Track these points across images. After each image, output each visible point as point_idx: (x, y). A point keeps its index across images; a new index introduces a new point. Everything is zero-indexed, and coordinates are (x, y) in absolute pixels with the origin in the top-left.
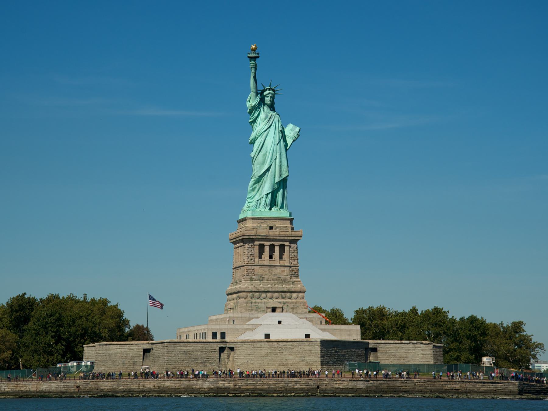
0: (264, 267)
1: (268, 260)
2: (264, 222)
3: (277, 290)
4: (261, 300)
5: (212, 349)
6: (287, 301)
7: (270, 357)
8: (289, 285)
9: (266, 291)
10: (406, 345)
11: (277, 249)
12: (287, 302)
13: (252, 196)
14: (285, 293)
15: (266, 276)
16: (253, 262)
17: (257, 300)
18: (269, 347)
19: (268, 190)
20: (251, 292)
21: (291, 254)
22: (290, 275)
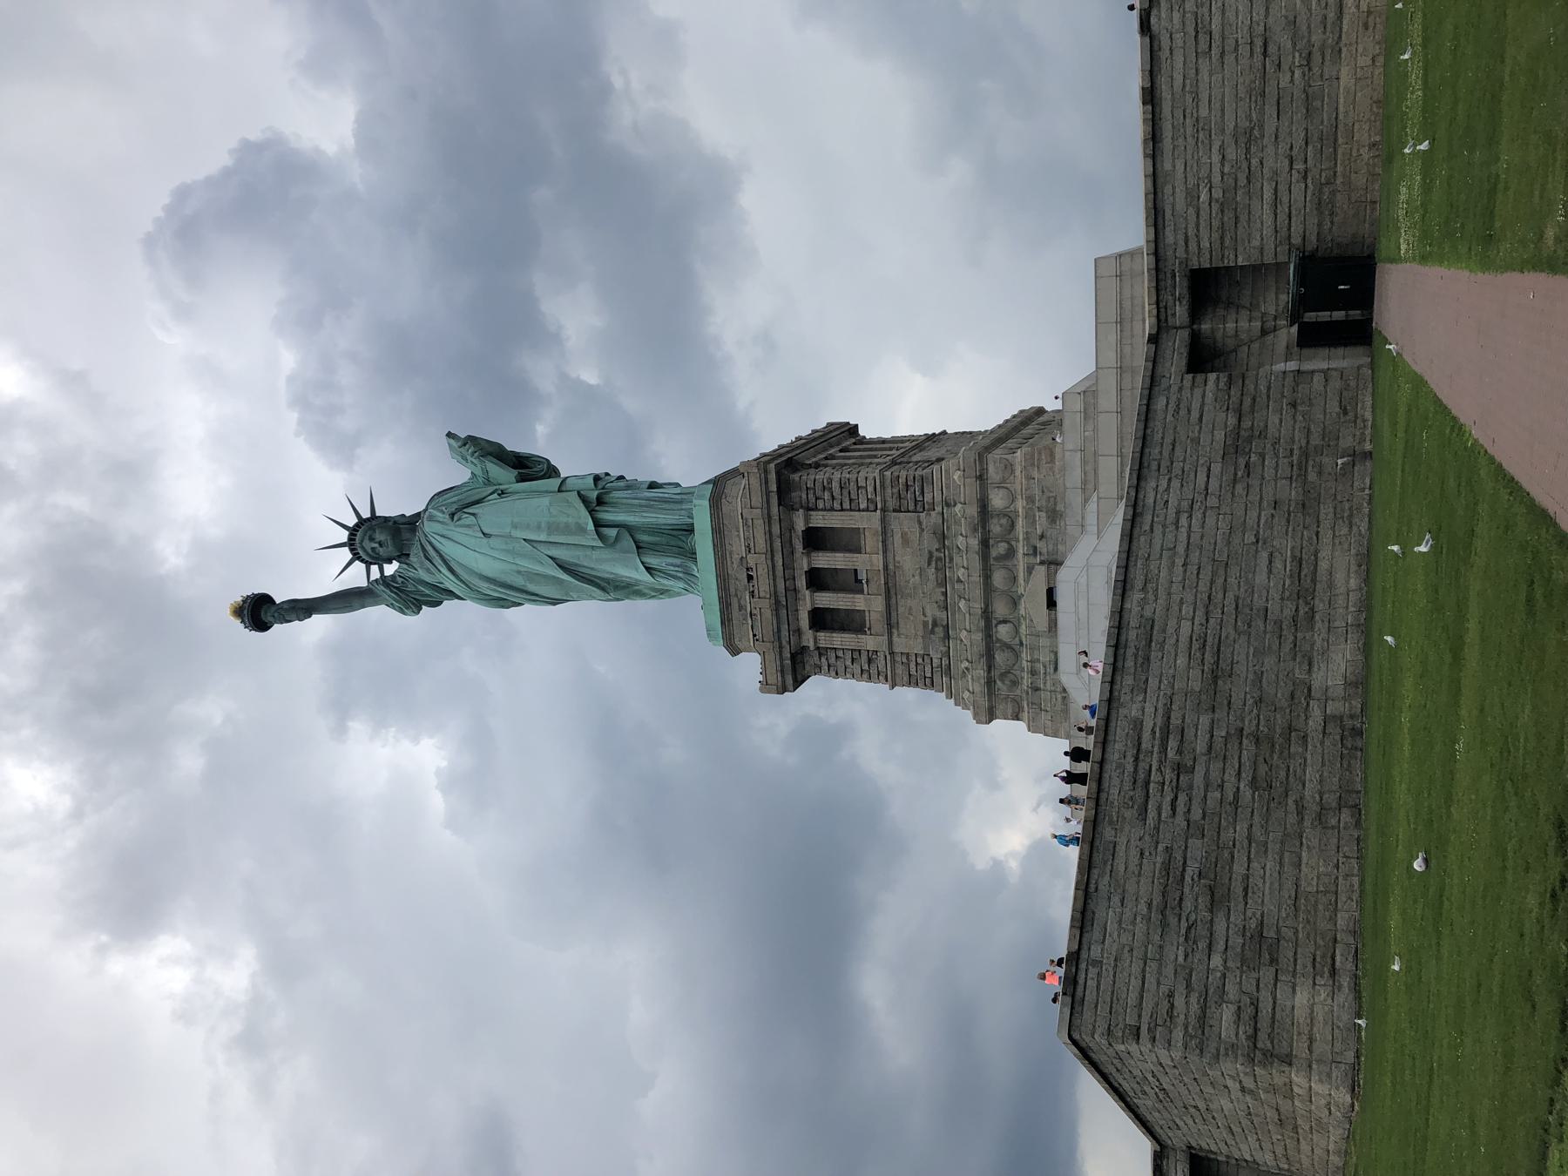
0: (894, 614)
1: (865, 600)
3: (976, 577)
4: (1021, 644)
6: (1021, 538)
9: (982, 623)
10: (1164, 54)
11: (823, 560)
12: (1027, 539)
15: (929, 613)
16: (881, 655)
17: (1025, 664)
19: (637, 570)
20: (990, 682)
21: (837, 505)
22: (918, 506)
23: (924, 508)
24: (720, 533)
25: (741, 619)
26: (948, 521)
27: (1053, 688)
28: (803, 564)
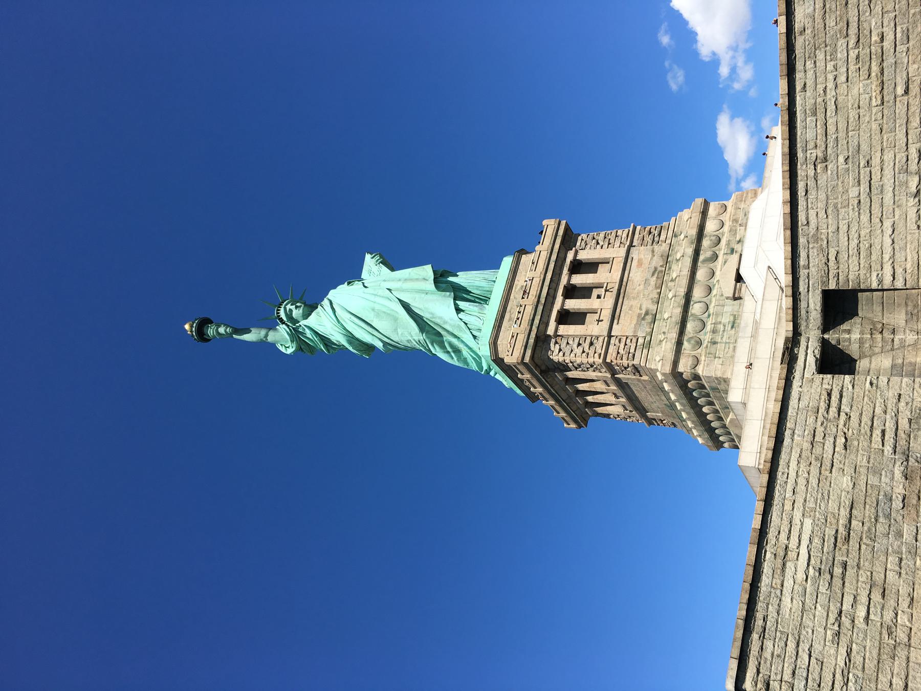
0: (618, 310)
1: (601, 302)
2: (511, 314)
3: (686, 272)
5: (823, 406)
6: (723, 248)
7: (889, 37)
8: (679, 244)
9: (683, 301)
11: (579, 279)
13: (471, 355)
14: (701, 252)
16: (601, 339)
17: (709, 327)
18: (820, 56)
19: (449, 307)
20: (679, 344)
23: (658, 243)
24: (514, 273)
25: (508, 327)
26: (673, 245)
27: (727, 341)
28: (564, 280)
